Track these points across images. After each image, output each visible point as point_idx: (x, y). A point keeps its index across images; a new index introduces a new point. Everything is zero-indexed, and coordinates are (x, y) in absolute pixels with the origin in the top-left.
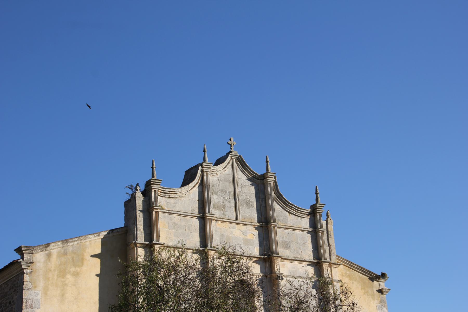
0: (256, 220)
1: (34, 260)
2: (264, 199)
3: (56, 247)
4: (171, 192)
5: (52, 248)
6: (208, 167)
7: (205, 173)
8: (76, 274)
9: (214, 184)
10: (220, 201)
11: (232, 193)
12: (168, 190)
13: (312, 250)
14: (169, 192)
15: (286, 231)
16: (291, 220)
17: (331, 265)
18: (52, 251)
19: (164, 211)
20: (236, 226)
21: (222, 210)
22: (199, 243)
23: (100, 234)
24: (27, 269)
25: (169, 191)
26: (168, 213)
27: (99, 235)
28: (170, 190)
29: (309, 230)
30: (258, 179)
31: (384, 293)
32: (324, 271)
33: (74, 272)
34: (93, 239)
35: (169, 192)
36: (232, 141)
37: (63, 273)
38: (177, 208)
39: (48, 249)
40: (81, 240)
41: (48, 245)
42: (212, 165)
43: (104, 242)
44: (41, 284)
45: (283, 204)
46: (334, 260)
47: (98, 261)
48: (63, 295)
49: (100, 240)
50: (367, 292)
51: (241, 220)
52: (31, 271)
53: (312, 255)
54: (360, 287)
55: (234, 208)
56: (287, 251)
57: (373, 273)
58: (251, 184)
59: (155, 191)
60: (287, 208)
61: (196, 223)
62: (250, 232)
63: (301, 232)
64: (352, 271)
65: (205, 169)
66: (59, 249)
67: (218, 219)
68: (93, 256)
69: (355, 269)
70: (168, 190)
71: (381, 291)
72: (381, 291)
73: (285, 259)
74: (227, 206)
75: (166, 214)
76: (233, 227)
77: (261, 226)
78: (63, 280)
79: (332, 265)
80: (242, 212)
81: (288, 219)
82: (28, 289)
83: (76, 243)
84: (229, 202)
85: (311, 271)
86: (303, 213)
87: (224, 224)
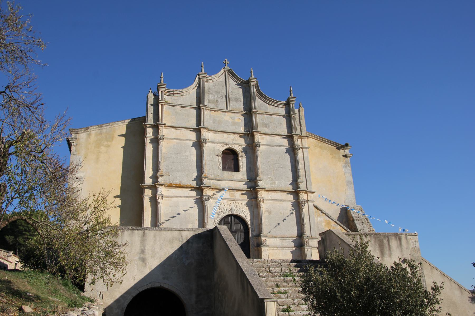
0: (243, 110)
1: (79, 138)
2: (249, 97)
3: (94, 129)
4: (174, 92)
5: (91, 130)
6: (203, 75)
7: (201, 80)
8: (108, 146)
9: (210, 87)
11: (225, 93)
12: (172, 91)
13: (287, 128)
14: (173, 92)
15: (266, 116)
16: (270, 109)
17: (301, 137)
18: (91, 132)
19: (169, 104)
20: (226, 114)
21: (216, 104)
22: (195, 124)
23: (125, 122)
24: (73, 143)
25: (173, 92)
26: (172, 105)
27: (124, 122)
28: (173, 91)
29: (284, 115)
30: (245, 84)
31: (348, 157)
32: (295, 141)
33: (106, 145)
34: (121, 124)
35: (173, 92)
36: (226, 61)
37: (98, 145)
38: (179, 102)
39: (88, 131)
40: (112, 125)
41: (87, 128)
42: (206, 74)
43: (128, 127)
44: (83, 152)
45: (263, 99)
46: (304, 133)
47: (123, 139)
48: (98, 158)
49: (126, 125)
50: (335, 157)
51: (230, 110)
52: (77, 144)
53: (287, 131)
54: (329, 154)
55: (225, 103)
57: (339, 144)
58: (239, 88)
59: (162, 92)
60: (267, 101)
61: (194, 112)
62: (237, 117)
63: (278, 116)
64: (323, 143)
65: (201, 77)
66: (97, 131)
67: (212, 109)
68: (119, 136)
69: (325, 142)
70: (172, 91)
71: (345, 156)
72: (345, 156)
73: (264, 134)
74: (220, 101)
75: (171, 107)
76: (224, 114)
77: (246, 113)
78: (98, 149)
79: (302, 137)
80: (231, 105)
81: (268, 109)
82: (74, 155)
83: (108, 127)
84: (222, 98)
85: (285, 142)
86: (280, 104)
87: (217, 112)
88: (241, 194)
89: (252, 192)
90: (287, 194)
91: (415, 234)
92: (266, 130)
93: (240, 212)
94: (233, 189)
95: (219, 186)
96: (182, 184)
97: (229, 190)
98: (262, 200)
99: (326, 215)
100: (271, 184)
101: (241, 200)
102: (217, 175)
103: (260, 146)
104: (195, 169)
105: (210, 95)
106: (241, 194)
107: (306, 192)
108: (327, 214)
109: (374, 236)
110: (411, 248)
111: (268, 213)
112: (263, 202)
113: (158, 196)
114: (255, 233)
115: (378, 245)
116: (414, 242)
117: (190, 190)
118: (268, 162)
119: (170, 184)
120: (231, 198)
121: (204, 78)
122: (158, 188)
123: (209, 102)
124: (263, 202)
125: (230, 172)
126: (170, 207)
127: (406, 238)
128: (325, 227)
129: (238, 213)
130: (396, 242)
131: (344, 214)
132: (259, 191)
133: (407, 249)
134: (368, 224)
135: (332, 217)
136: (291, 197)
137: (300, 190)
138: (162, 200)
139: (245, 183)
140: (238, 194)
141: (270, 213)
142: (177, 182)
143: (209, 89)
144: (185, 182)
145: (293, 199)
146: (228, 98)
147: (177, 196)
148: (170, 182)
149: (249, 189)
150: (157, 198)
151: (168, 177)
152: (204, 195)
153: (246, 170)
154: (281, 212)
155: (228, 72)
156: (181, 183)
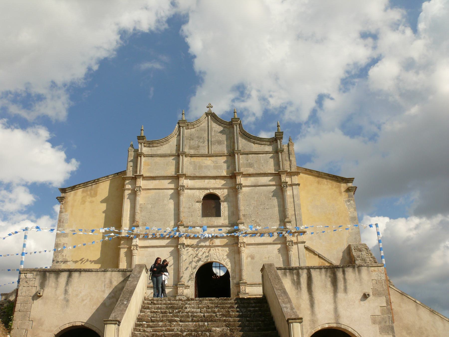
10: (196, 144)
20: (208, 158)
30: (229, 125)
38: (159, 152)
55: (207, 147)
56: (251, 169)
63: (264, 155)
66: (83, 188)
81: (253, 147)
92: (251, 171)
102: (196, 222)
103: (241, 188)
104: (172, 217)
105: (192, 142)
108: (320, 255)
113: (132, 247)
114: (235, 281)
116: (379, 274)
118: (253, 203)
121: (184, 125)
123: (190, 148)
125: (210, 218)
126: (146, 257)
135: (326, 258)
138: (136, 251)
141: (253, 258)
143: (191, 135)
146: (210, 142)
150: (132, 249)
153: (227, 214)
154: (266, 256)
155: (210, 116)
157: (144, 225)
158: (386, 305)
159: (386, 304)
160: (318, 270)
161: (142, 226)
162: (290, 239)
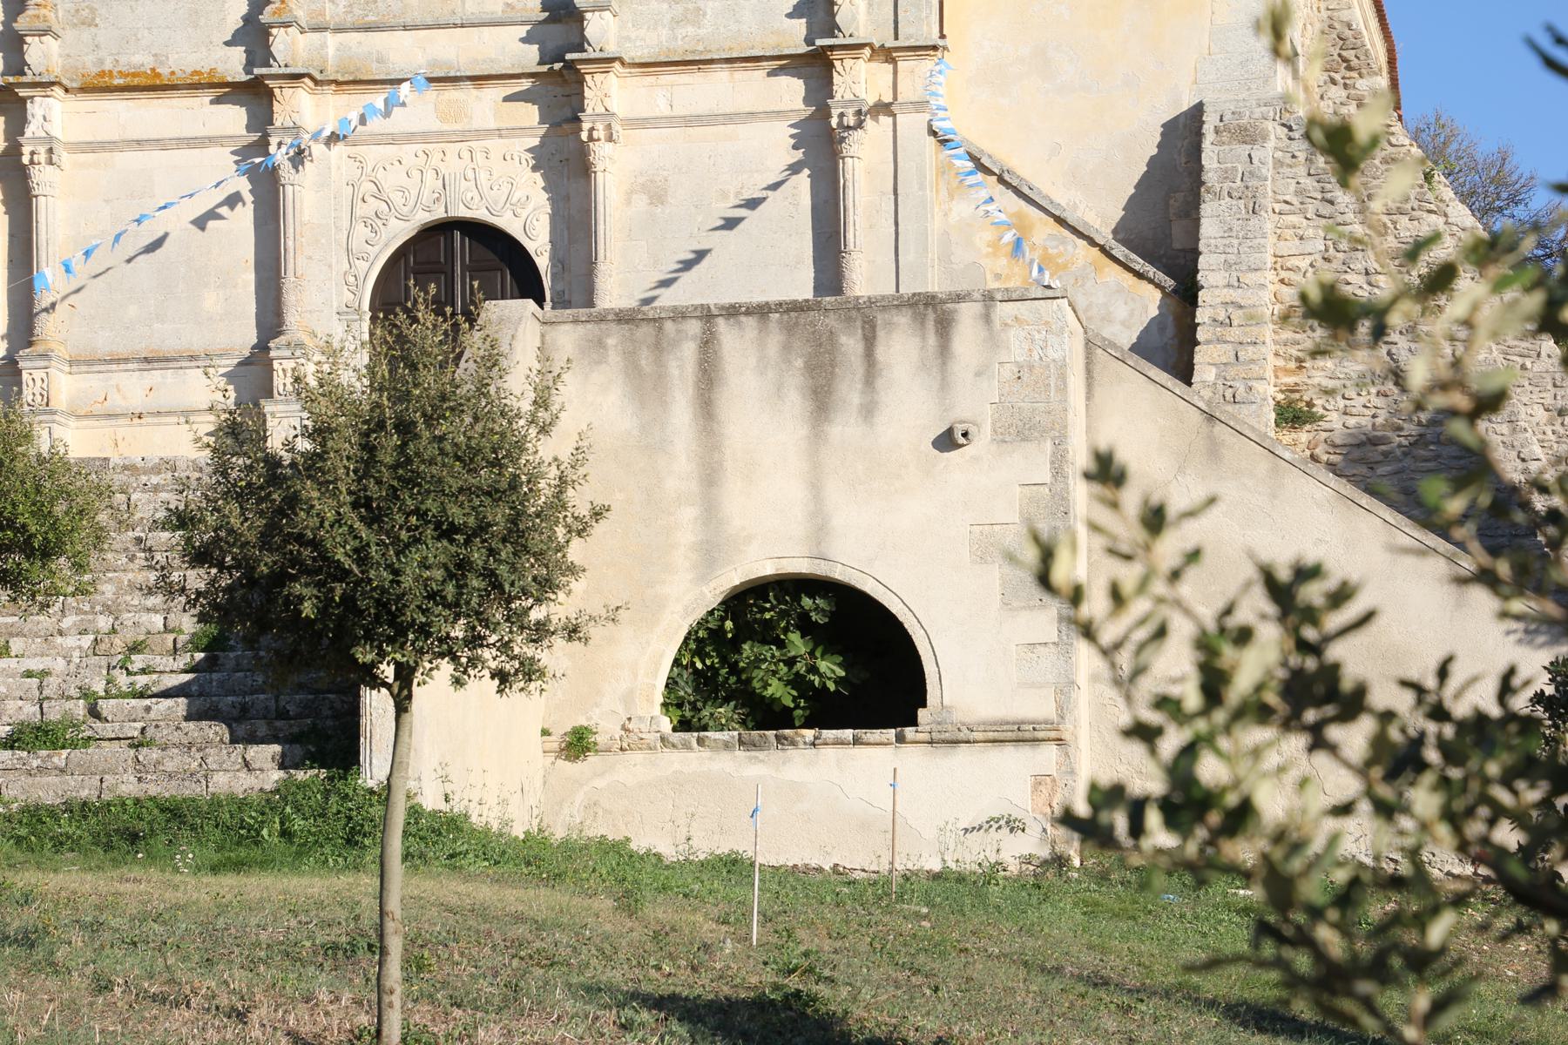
88: (507, 99)
89: (565, 81)
90: (769, 75)
91: (1049, 293)
93: (496, 203)
94: (452, 74)
95: (374, 65)
96: (164, 71)
97: (431, 80)
98: (600, 126)
99: (1001, 180)
100: (676, 22)
101: (500, 136)
106: (507, 99)
107: (886, 54)
108: (1007, 177)
109: (786, 317)
110: (1008, 372)
111: (651, 198)
112: (610, 139)
113: (26, 150)
115: (799, 363)
117: (212, 102)
119: (102, 74)
120: (446, 127)
122: (29, 105)
124: (610, 139)
126: (107, 201)
127: (987, 318)
128: (988, 255)
129: (480, 213)
130: (918, 339)
131: (1183, 160)
132: (588, 77)
133: (978, 374)
134: (1326, 210)
135: (1040, 193)
136: (791, 92)
137: (832, 48)
139: (528, 32)
140: (485, 105)
141: (658, 196)
142: (140, 59)
144: (185, 59)
145: (807, 101)
147: (138, 142)
148: (101, 62)
149: (545, 68)
150: (25, 160)
151: (86, 34)
152: (278, 124)
156: (162, 63)
157: (83, 24)
158: (1047, 478)
159: (1050, 475)
160: (750, 322)
161: (76, 25)
162: (848, 90)
